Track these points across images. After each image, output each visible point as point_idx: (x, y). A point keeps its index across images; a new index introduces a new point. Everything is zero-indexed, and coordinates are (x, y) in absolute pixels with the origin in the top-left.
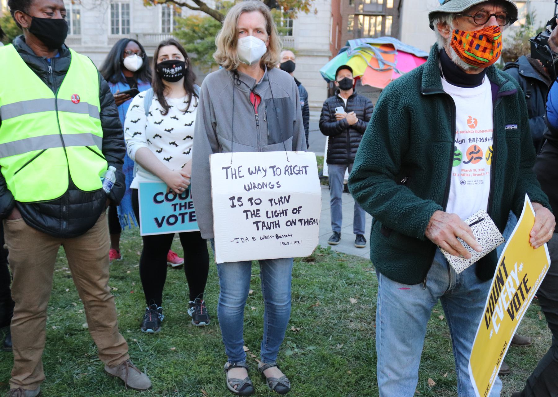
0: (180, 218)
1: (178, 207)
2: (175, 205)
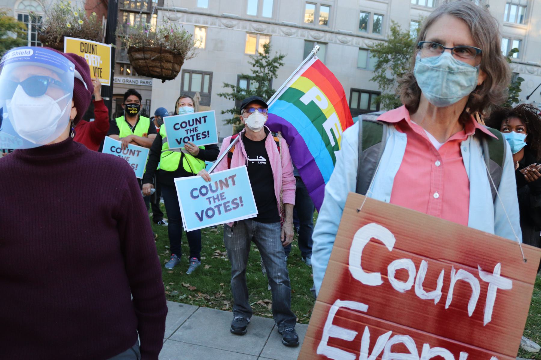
0: (216, 210)
1: (212, 200)
2: (209, 199)
